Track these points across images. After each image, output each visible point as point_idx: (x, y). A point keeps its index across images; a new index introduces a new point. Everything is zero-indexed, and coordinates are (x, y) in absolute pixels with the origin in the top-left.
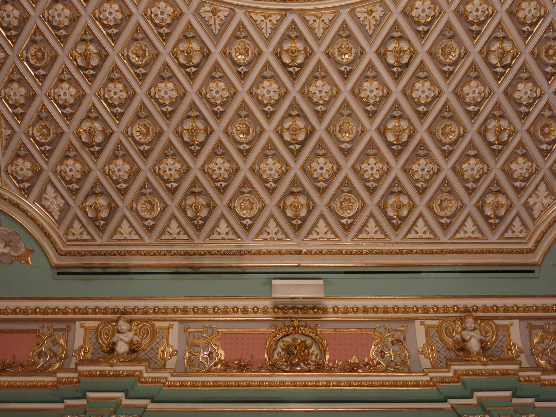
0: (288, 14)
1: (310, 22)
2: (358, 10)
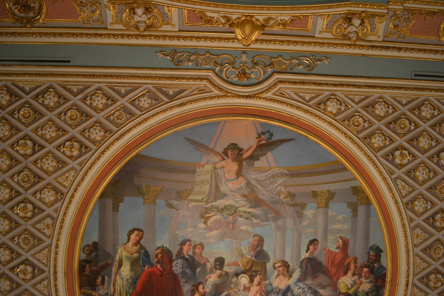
0: (414, 283)
1: (420, 270)
2: (415, 243)
